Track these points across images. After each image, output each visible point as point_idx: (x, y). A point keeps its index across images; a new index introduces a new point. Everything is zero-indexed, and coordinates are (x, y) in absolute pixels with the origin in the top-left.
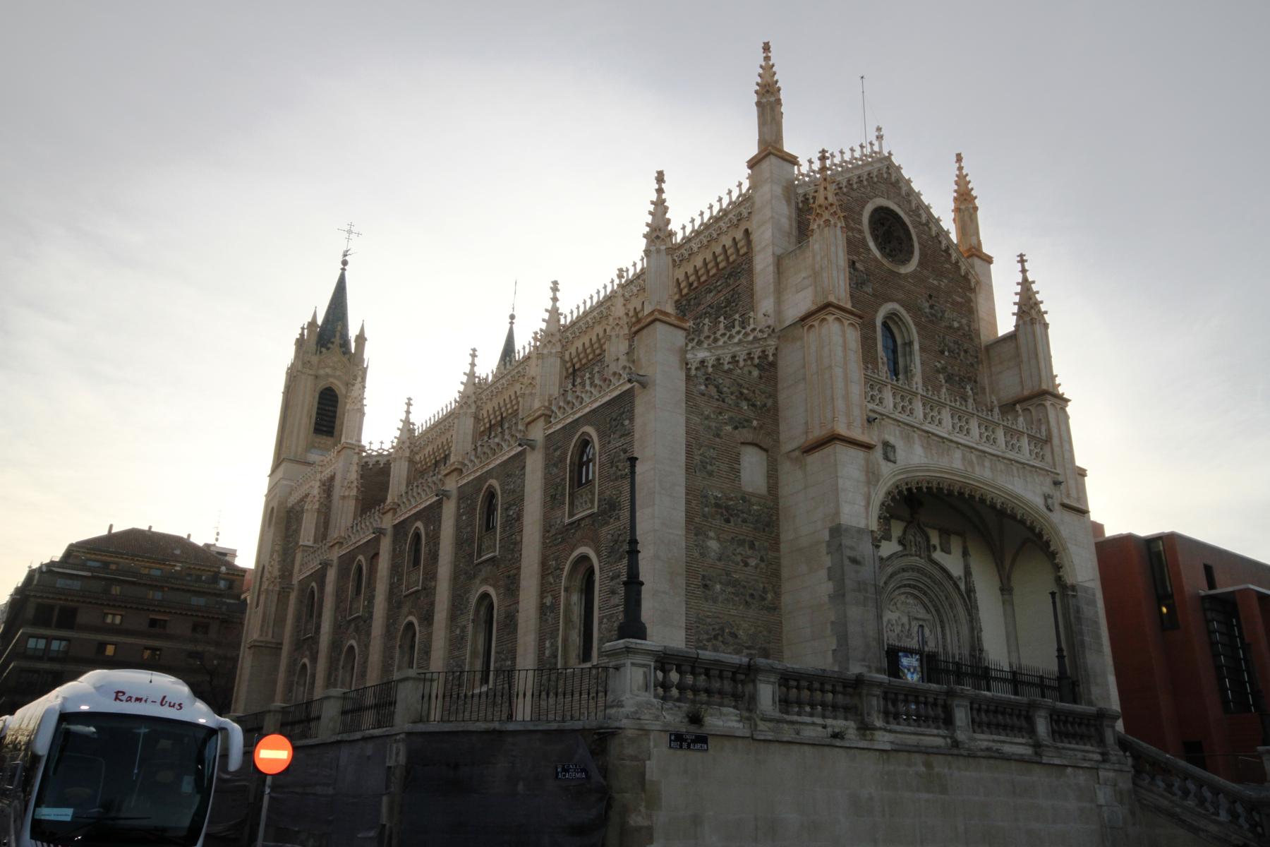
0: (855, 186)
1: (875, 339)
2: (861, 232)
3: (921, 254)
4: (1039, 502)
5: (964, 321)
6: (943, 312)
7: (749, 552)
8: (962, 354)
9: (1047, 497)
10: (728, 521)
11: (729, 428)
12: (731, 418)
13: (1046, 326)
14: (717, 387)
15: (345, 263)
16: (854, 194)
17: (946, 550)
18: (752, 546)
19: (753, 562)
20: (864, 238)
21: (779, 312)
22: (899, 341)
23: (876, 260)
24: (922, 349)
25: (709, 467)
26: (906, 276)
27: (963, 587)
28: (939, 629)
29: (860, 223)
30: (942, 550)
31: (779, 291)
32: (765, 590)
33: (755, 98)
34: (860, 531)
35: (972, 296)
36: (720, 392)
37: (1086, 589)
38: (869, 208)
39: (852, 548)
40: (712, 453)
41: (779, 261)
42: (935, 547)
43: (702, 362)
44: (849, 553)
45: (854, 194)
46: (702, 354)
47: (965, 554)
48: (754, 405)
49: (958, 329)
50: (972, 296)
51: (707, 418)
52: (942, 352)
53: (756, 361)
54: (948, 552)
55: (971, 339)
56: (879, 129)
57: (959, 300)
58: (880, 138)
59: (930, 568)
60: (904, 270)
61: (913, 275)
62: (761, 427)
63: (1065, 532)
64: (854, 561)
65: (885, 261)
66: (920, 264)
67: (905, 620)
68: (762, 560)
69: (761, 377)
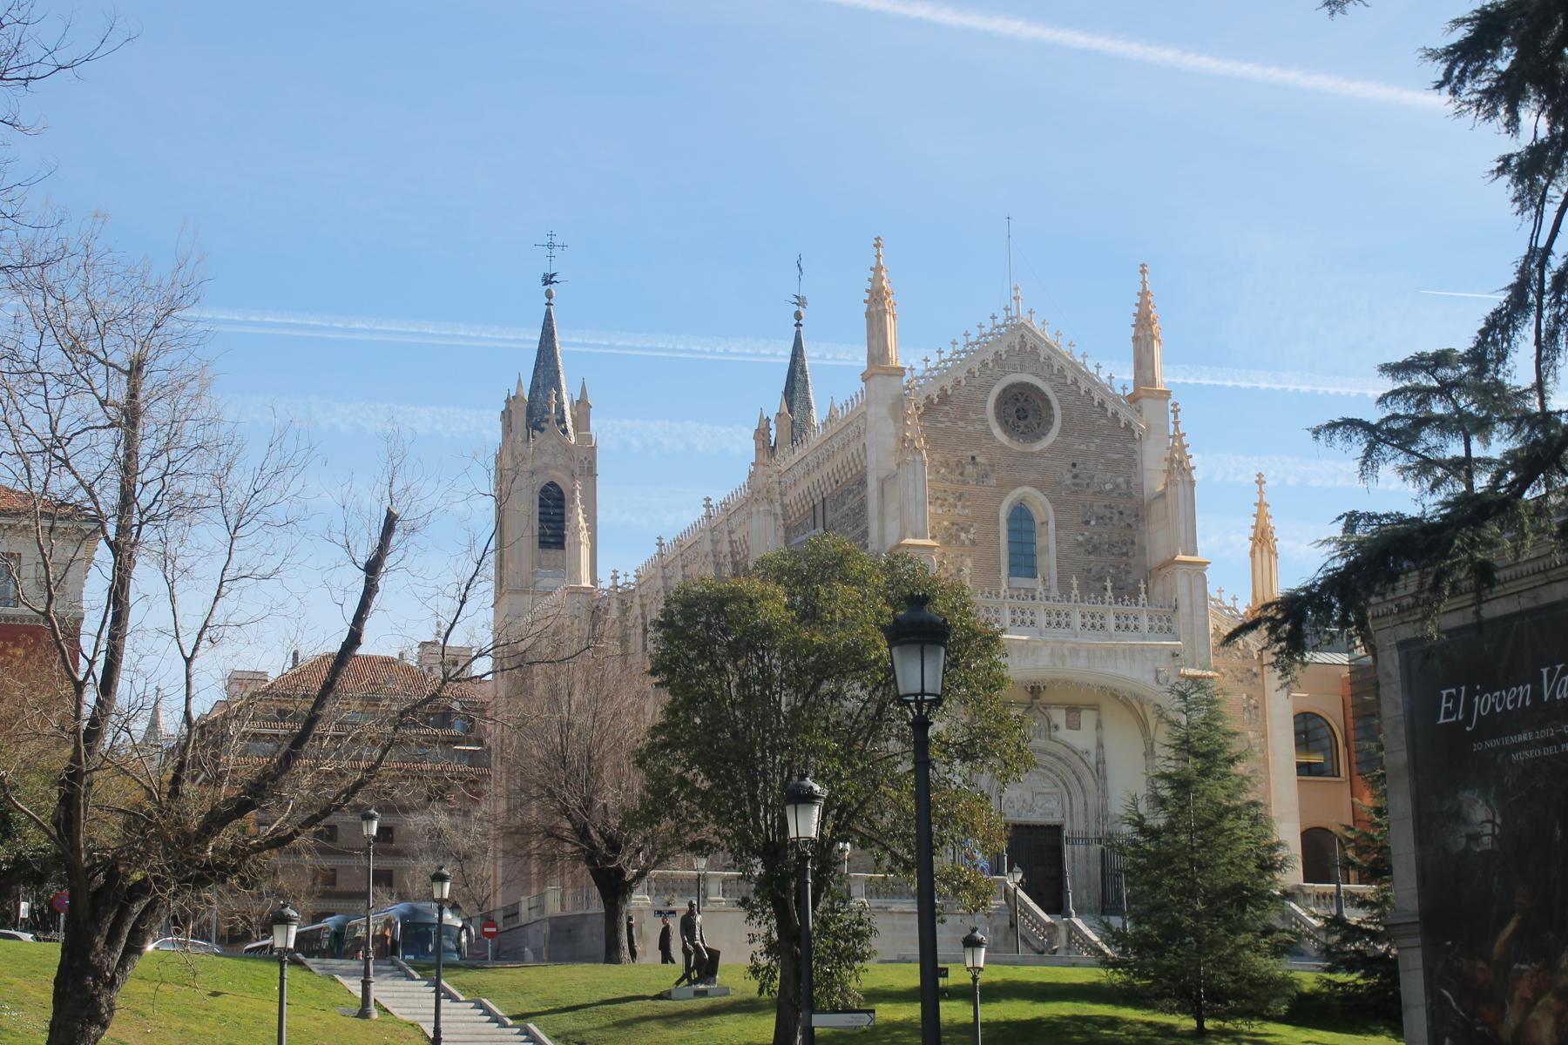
1: (998, 532)
2: (984, 421)
5: (1120, 480)
6: (1091, 478)
8: (1116, 517)
9: (1157, 672)
13: (1192, 483)
17: (1074, 725)
20: (988, 428)
21: (882, 537)
22: (1037, 521)
23: (1002, 446)
27: (1092, 760)
28: (1067, 800)
29: (984, 412)
30: (1069, 727)
31: (882, 514)
35: (1136, 447)
38: (997, 390)
41: (882, 483)
42: (1056, 727)
45: (975, 382)
47: (1099, 726)
49: (1112, 491)
50: (1136, 447)
52: (1087, 523)
55: (1130, 496)
56: (1016, 289)
57: (1116, 456)
59: (1052, 747)
61: (1051, 449)
65: (1016, 446)
66: (1063, 431)
67: (1028, 796)
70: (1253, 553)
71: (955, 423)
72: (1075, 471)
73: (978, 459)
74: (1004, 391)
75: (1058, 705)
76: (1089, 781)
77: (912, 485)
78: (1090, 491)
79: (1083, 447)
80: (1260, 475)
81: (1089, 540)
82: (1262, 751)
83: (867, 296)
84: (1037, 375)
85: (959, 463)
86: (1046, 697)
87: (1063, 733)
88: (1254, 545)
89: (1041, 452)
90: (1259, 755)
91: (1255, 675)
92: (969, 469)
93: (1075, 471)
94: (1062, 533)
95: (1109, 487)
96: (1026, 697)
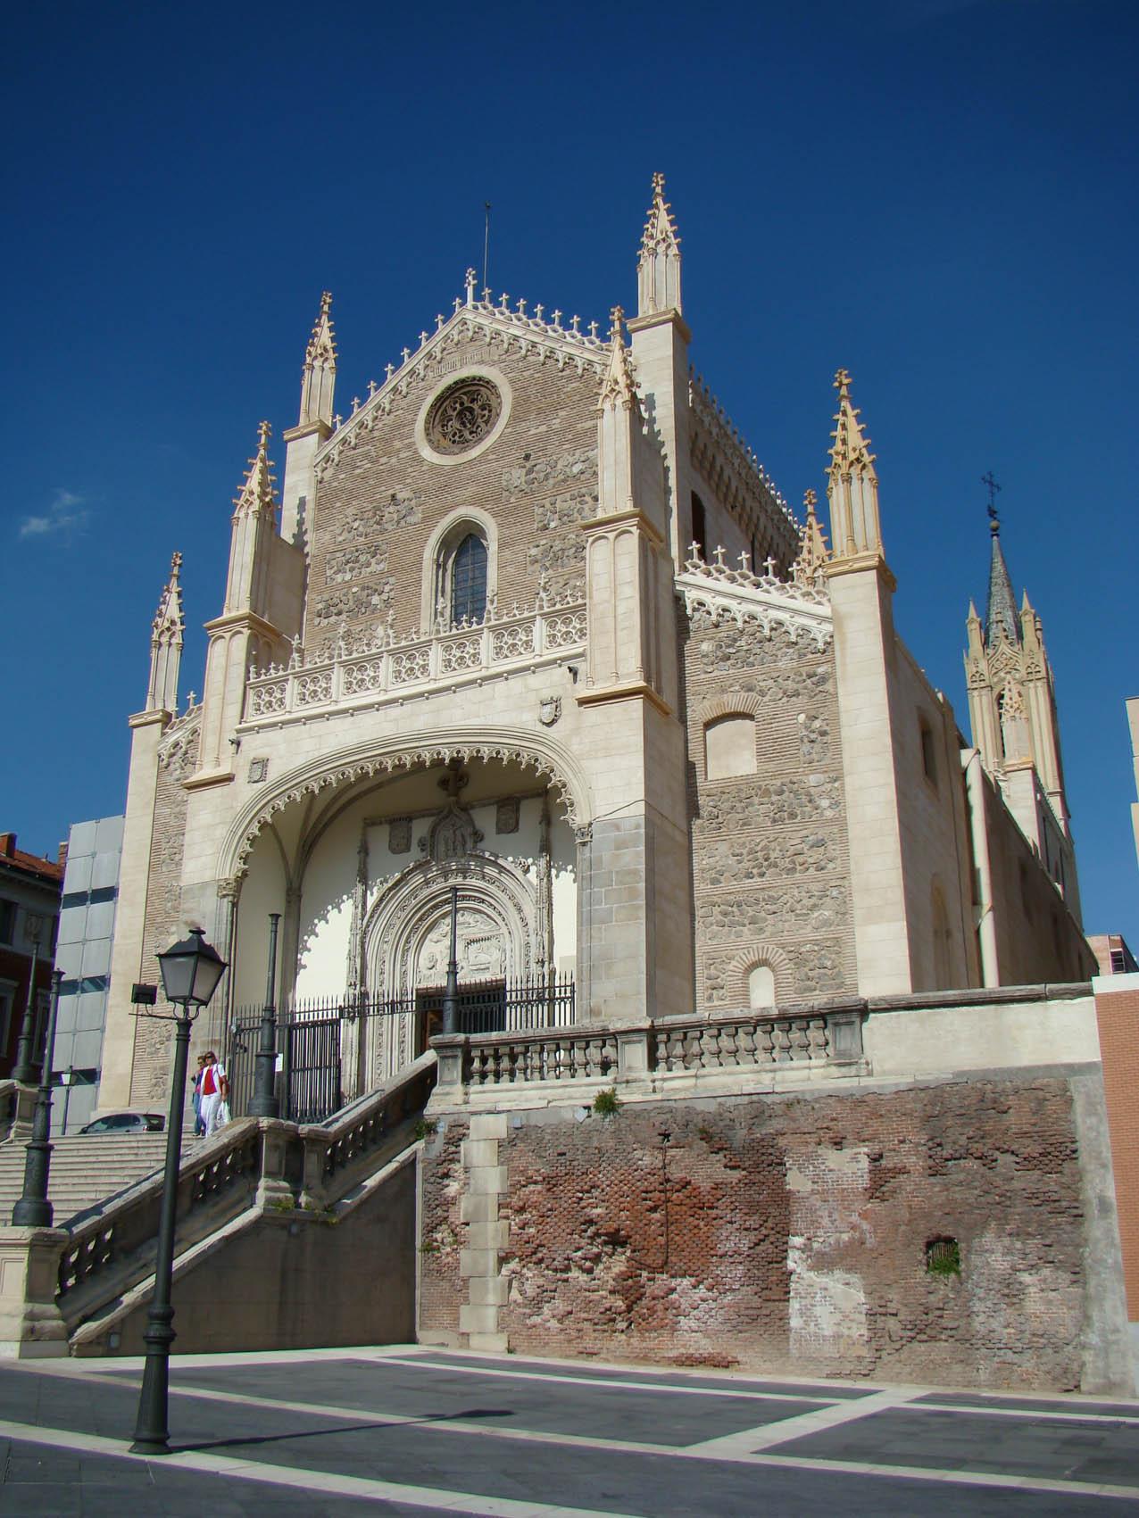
0: (405, 390)
1: (419, 581)
2: (410, 446)
3: (514, 408)
4: (528, 719)
16: (403, 404)
20: (416, 452)
23: (433, 467)
24: (502, 546)
30: (499, 831)
34: (204, 885)
43: (176, 745)
46: (172, 739)
52: (545, 528)
54: (515, 829)
60: (475, 452)
63: (575, 747)
66: (515, 418)
71: (374, 461)
72: (528, 465)
73: (400, 496)
74: (441, 399)
75: (484, 803)
76: (530, 910)
78: (551, 481)
79: (543, 428)
81: (545, 553)
82: (836, 804)
84: (482, 362)
85: (377, 509)
86: (468, 794)
89: (484, 454)
91: (823, 680)
92: (390, 512)
93: (528, 465)
94: (507, 553)
95: (576, 469)
96: (438, 797)
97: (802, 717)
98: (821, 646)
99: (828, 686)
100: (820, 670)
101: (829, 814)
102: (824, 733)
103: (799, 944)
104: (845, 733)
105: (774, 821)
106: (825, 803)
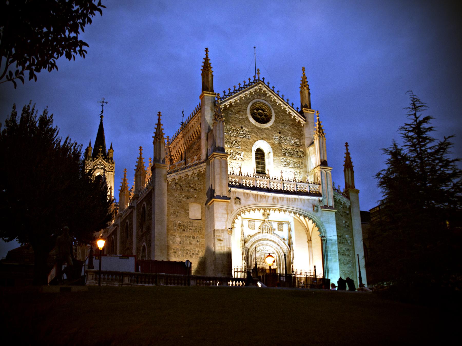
7: (192, 240)
10: (184, 230)
11: (185, 199)
12: (185, 196)
14: (180, 185)
15: (102, 117)
18: (193, 237)
19: (194, 242)
20: (247, 118)
25: (176, 213)
26: (267, 129)
30: (279, 230)
32: (198, 251)
33: (201, 71)
35: (302, 129)
36: (181, 187)
37: (331, 240)
39: (219, 236)
40: (178, 208)
44: (218, 238)
47: (290, 230)
48: (195, 189)
50: (302, 129)
51: (176, 197)
53: (196, 174)
54: (282, 230)
56: (258, 70)
58: (258, 73)
62: (198, 197)
64: (220, 240)
66: (275, 122)
68: (197, 241)
69: (198, 179)
70: (345, 171)
77: (218, 132)
80: (347, 143)
82: (351, 242)
83: (202, 68)
87: (277, 232)
88: (345, 168)
90: (350, 244)
91: (348, 214)
97: (344, 222)
98: (348, 207)
99: (349, 216)
100: (348, 212)
101: (350, 244)
102: (348, 226)
103: (345, 271)
104: (354, 227)
105: (339, 243)
106: (349, 242)
